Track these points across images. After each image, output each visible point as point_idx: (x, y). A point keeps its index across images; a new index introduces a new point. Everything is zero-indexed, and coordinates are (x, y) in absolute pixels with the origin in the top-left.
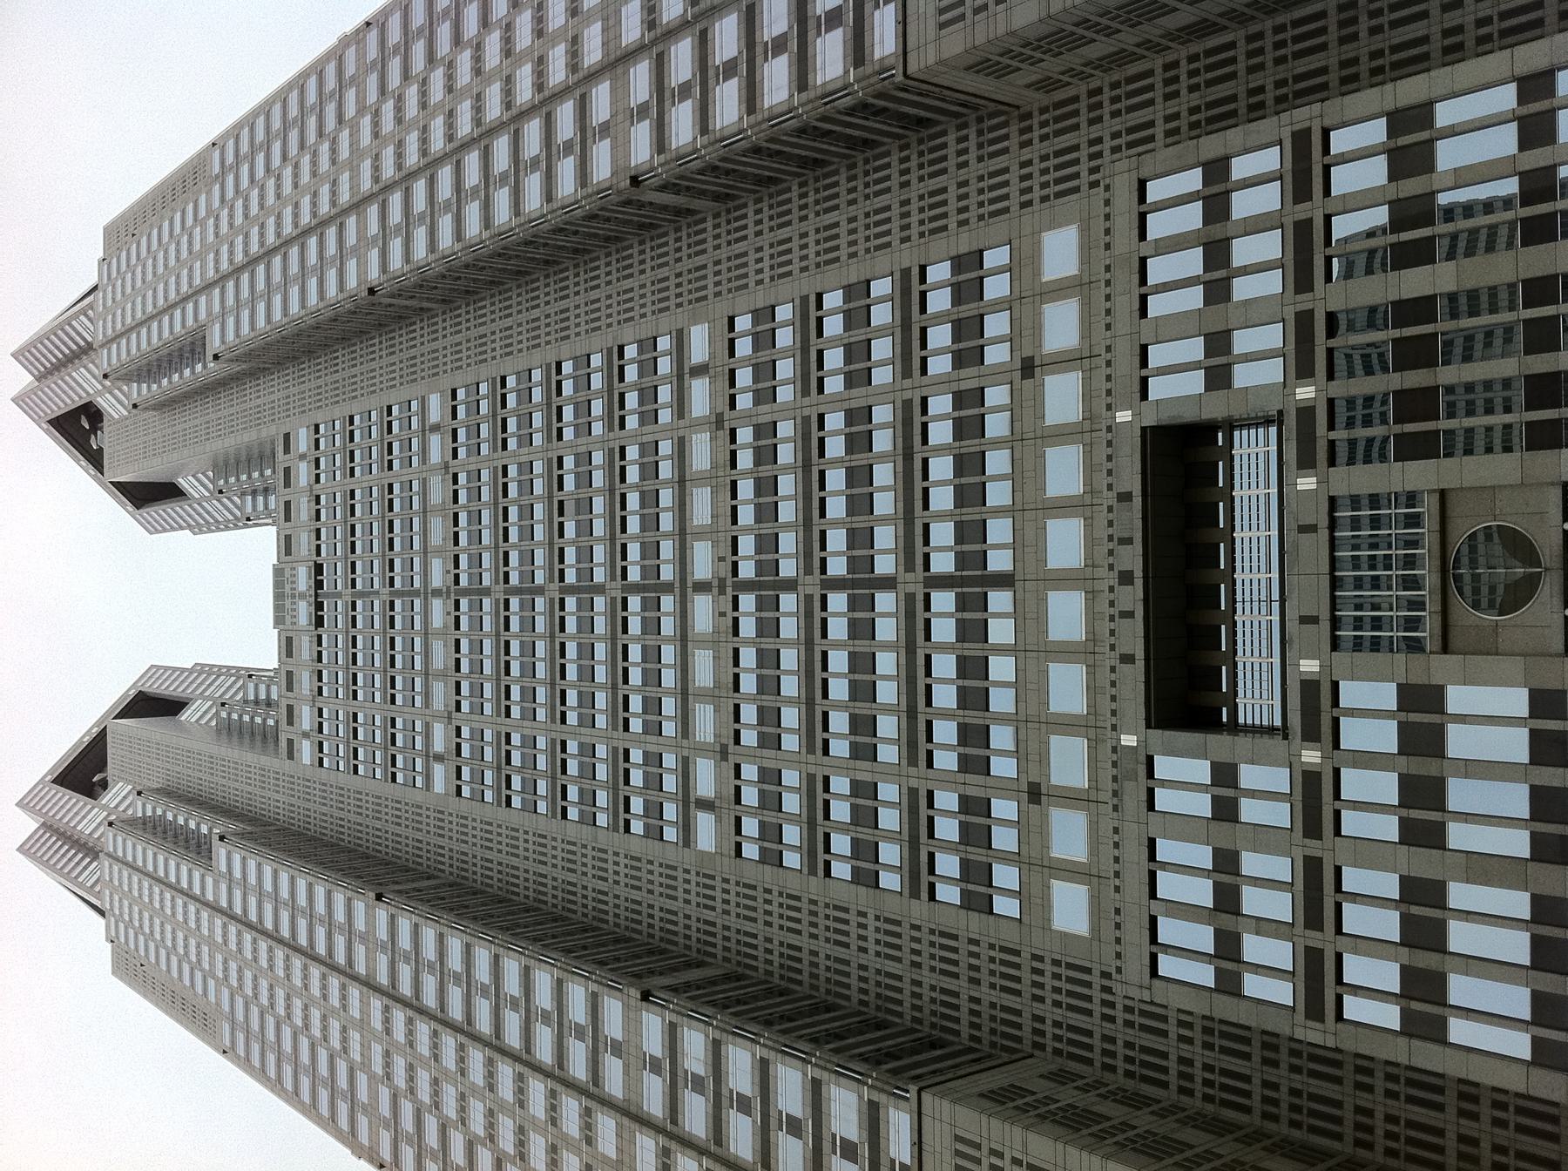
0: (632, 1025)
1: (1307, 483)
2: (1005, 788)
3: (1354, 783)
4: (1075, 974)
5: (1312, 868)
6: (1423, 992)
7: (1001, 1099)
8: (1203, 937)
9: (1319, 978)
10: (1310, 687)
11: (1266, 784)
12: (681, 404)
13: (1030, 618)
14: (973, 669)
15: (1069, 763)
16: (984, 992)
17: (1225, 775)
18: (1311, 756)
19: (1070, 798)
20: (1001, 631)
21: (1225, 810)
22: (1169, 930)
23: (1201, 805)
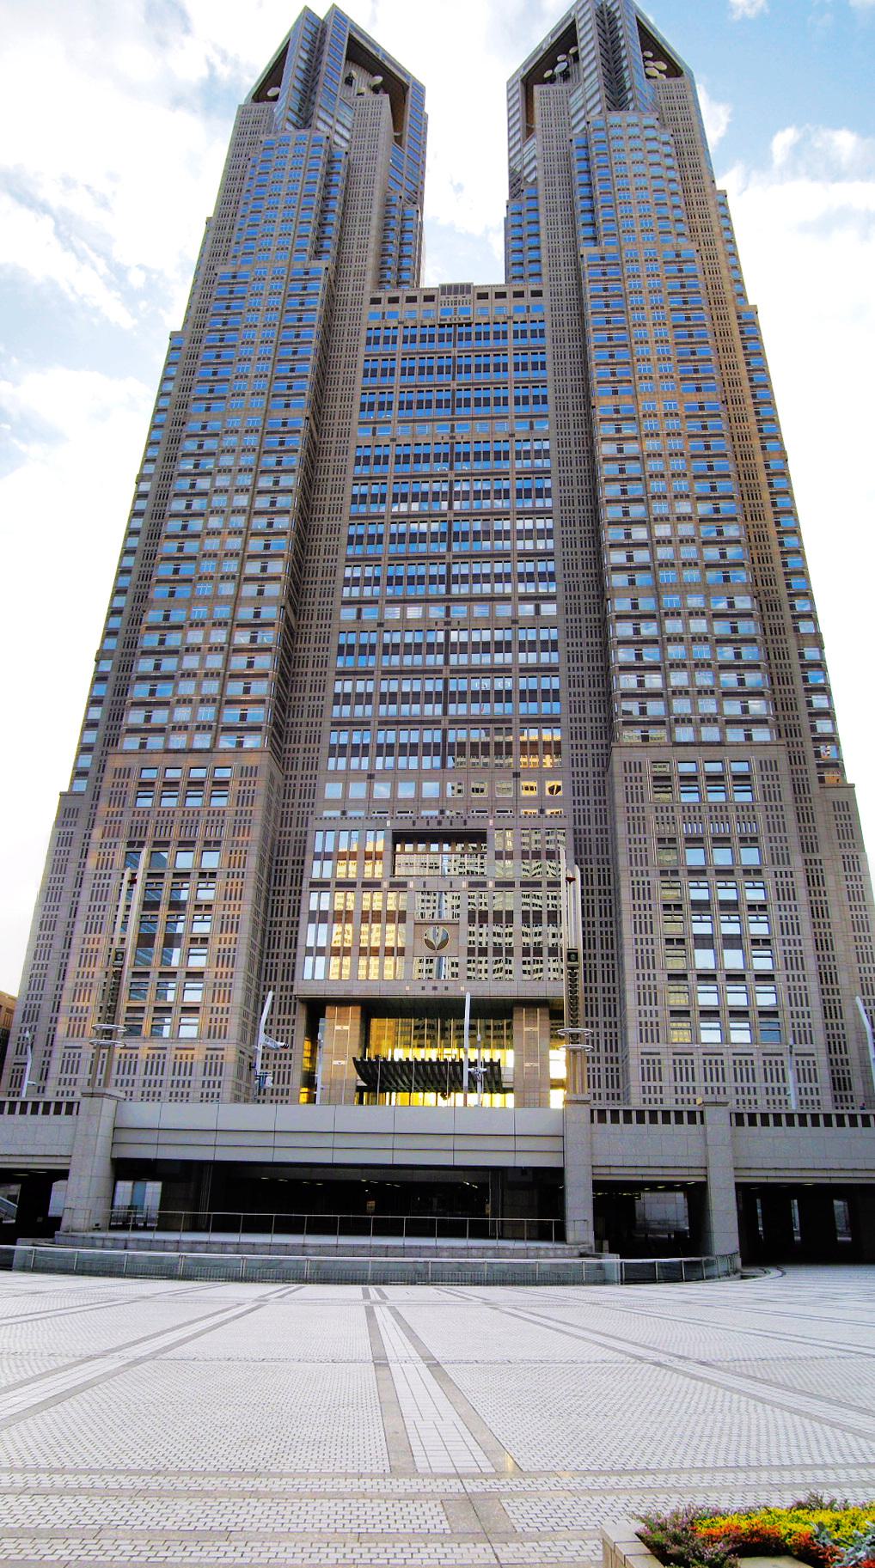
0: (271, 601)
1: (464, 885)
2: (372, 763)
3: (378, 896)
4: (312, 792)
5: (353, 885)
6: (321, 917)
7: (272, 779)
8: (330, 848)
9: (321, 885)
10: (404, 885)
11: (376, 870)
12: (525, 598)
13: (430, 775)
14: (411, 750)
15: (382, 790)
16: (301, 755)
17: (378, 856)
18: (385, 885)
19: (370, 791)
20: (427, 762)
21: (368, 856)
22: (331, 835)
23: (369, 848)
